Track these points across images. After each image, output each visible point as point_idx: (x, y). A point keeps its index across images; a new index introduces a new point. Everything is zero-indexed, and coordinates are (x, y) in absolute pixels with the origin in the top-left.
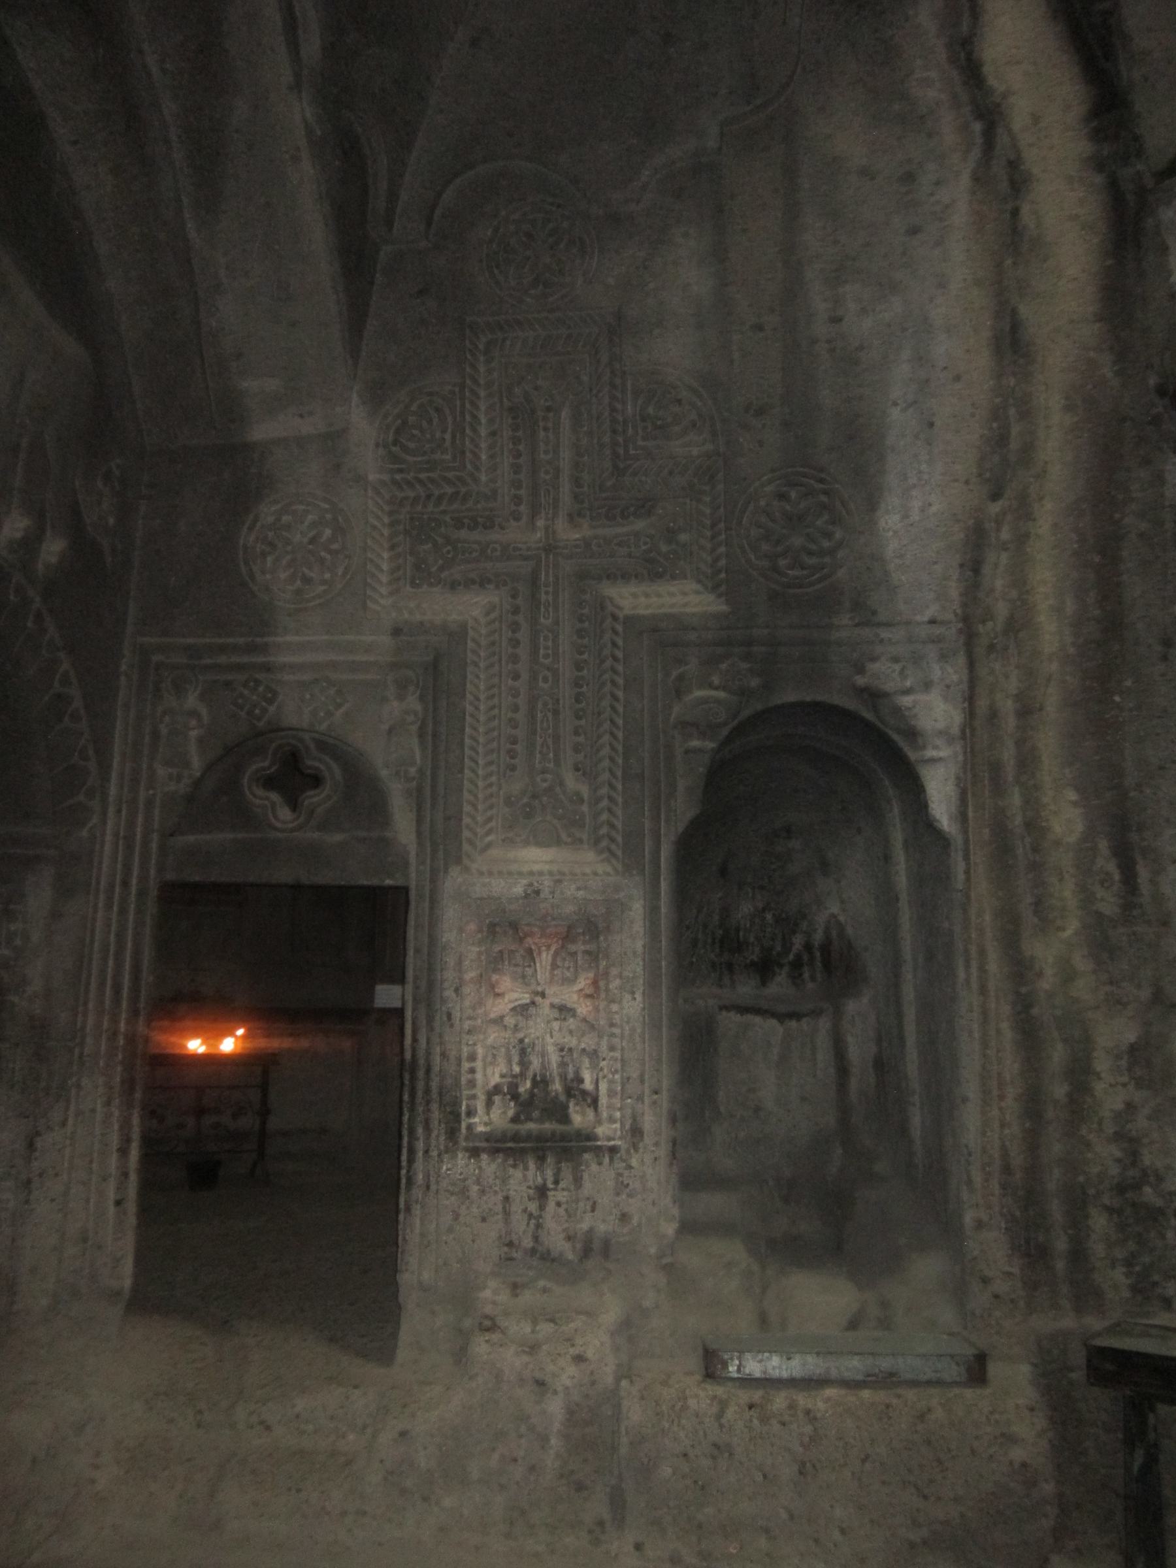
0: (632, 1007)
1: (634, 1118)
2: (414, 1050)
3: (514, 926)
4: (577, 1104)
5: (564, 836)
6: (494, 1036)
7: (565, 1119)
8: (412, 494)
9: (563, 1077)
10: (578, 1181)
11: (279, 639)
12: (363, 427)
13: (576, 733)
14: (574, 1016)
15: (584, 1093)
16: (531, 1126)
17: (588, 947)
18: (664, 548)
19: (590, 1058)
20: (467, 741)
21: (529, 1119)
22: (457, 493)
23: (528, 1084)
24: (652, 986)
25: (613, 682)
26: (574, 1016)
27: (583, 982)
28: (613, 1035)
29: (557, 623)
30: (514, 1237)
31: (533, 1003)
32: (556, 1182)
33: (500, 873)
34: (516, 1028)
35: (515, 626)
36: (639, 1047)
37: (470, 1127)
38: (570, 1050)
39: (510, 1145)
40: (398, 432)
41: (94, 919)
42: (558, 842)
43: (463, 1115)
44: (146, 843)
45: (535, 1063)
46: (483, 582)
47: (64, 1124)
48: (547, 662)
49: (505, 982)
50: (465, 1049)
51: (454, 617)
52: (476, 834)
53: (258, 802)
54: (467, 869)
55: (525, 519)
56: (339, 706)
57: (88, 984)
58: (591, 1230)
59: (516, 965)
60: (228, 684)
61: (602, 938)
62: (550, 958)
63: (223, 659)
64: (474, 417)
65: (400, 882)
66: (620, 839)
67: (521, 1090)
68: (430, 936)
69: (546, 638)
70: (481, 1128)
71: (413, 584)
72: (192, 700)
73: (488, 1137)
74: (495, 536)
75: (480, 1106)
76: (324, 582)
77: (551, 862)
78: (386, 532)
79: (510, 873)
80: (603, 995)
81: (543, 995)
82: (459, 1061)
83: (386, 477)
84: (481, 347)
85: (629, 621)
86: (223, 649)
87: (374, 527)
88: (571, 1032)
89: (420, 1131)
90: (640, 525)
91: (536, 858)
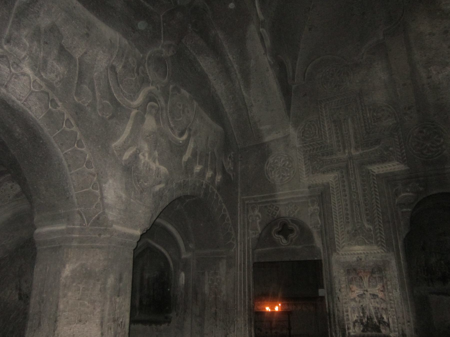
0: (397, 294)
2: (329, 310)
3: (355, 270)
5: (367, 241)
6: (353, 304)
7: (379, 331)
8: (309, 149)
9: (377, 317)
11: (278, 193)
12: (293, 133)
13: (366, 210)
15: (384, 322)
16: (369, 333)
18: (385, 153)
20: (334, 216)
21: (367, 330)
22: (321, 147)
23: (366, 319)
24: (402, 287)
25: (376, 194)
27: (379, 286)
28: (391, 303)
29: (356, 179)
31: (364, 294)
33: (348, 254)
34: (360, 302)
35: (343, 182)
37: (349, 333)
38: (378, 308)
40: (303, 133)
41: (237, 274)
42: (365, 244)
44: (248, 252)
45: (367, 313)
46: (332, 170)
47: (234, 331)
48: (354, 190)
49: (354, 288)
50: (345, 309)
51: (325, 181)
52: (339, 243)
53: (277, 238)
54: (338, 254)
55: (342, 150)
56: (296, 210)
57: (237, 292)
59: (357, 282)
60: (266, 207)
62: (368, 279)
63: (264, 200)
64: (324, 125)
65: (319, 259)
66: (385, 242)
67: (364, 321)
68: (330, 274)
69: (353, 184)
70: (352, 334)
71: (312, 173)
72: (257, 212)
74: (334, 157)
75: (351, 327)
76: (288, 176)
77: (364, 250)
78: (303, 160)
79: (351, 254)
80: (386, 290)
81: (367, 291)
82: (343, 312)
83: (301, 145)
84: (323, 106)
85: (378, 176)
86: (263, 198)
87: (300, 159)
88: (377, 303)
89: (334, 334)
90: (377, 147)
91: (359, 249)
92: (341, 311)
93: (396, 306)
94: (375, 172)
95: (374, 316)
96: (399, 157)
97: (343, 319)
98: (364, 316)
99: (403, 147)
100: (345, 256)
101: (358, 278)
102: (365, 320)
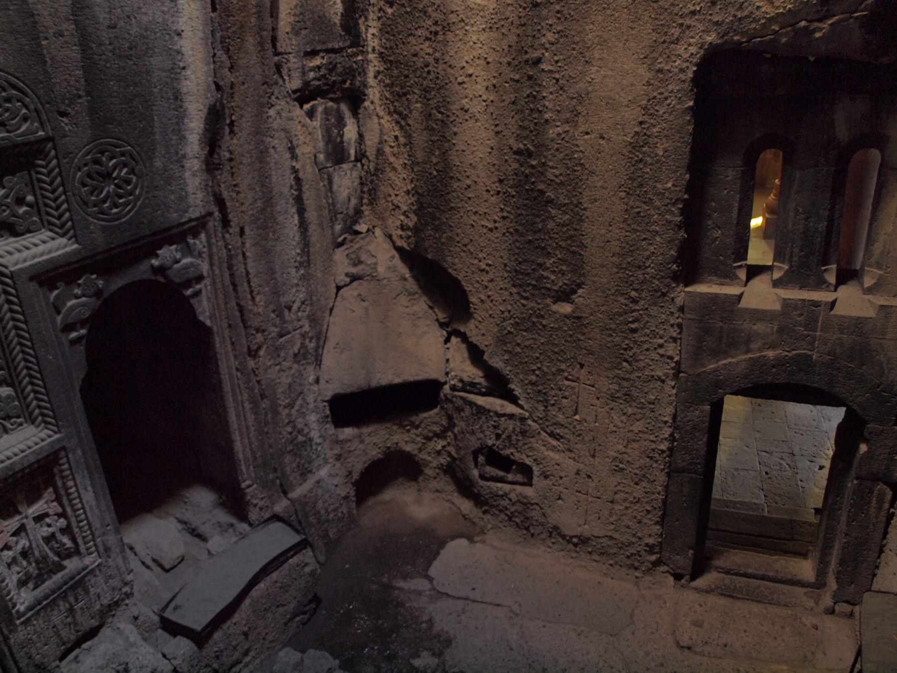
1: (104, 545)
5: (9, 426)
9: (52, 549)
10: (87, 592)
23: (34, 564)
30: (65, 639)
32: (77, 600)
37: (18, 611)
38: (53, 535)
39: (45, 603)
58: (102, 605)
67: (31, 570)
70: (22, 608)
73: (29, 609)
81: (26, 517)
88: (49, 526)
94: (6, 267)
96: (54, 220)
99: (63, 197)
102: (33, 569)
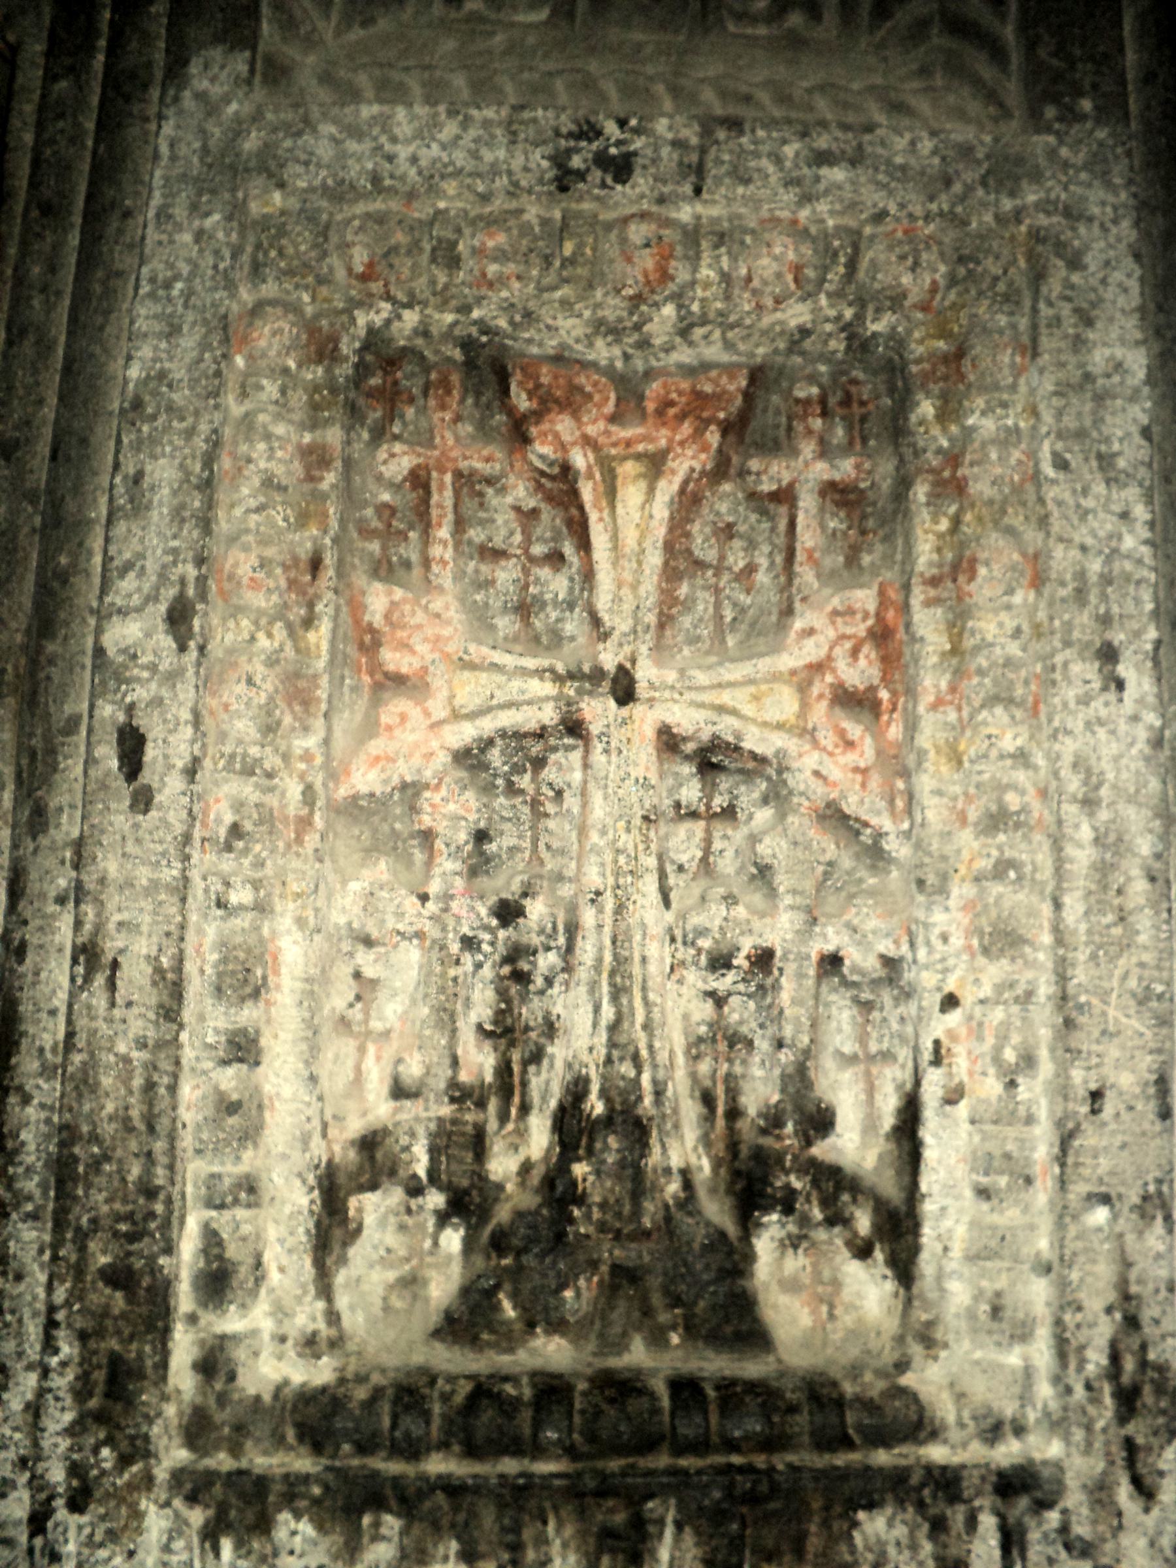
4: (793, 1243)
9: (719, 1104)
14: (778, 796)
15: (834, 1183)
16: (552, 1351)
17: (846, 468)
19: (867, 1007)
23: (539, 1138)
26: (778, 796)
27: (824, 630)
31: (574, 727)
36: (1145, 925)
37: (213, 1363)
38: (764, 959)
43: (184, 1298)
61: (926, 408)
62: (661, 510)
67: (502, 1165)
80: (932, 681)
81: (624, 690)
92: (135, 976)
93: (1074, 907)
95: (680, 1086)
97: (153, 1118)
98: (507, 1084)
100: (367, 111)
101: (520, 492)
102: (518, 1153)
